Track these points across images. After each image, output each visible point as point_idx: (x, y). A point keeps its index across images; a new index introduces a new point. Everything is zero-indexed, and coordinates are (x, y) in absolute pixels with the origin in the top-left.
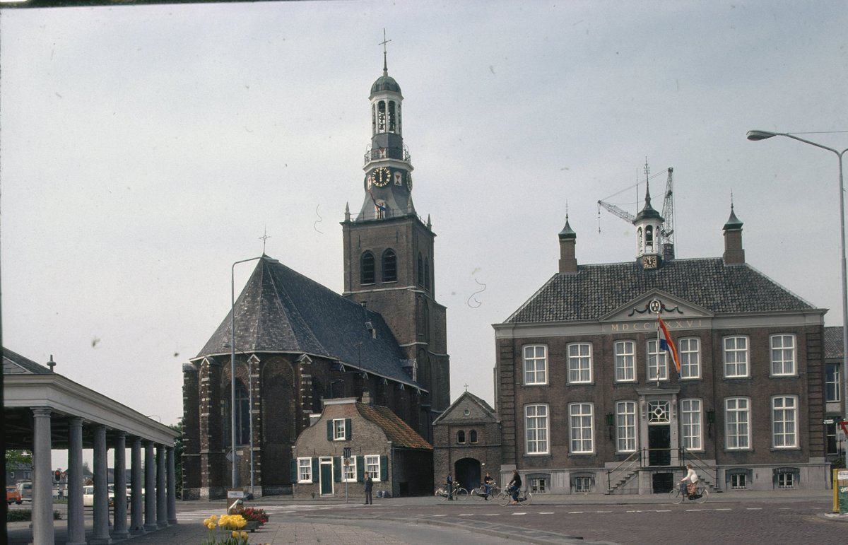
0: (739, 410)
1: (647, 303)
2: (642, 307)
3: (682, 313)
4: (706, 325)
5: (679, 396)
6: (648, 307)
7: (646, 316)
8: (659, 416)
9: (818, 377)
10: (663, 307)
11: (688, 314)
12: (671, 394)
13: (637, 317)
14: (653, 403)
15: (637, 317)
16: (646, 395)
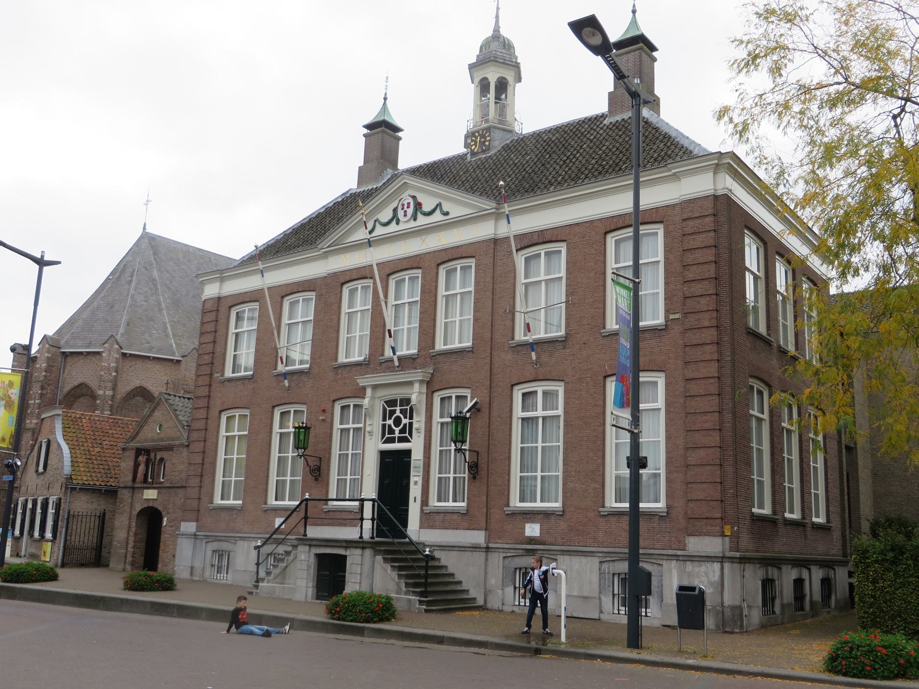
0: (538, 415)
1: (394, 205)
2: (385, 215)
3: (447, 214)
4: (484, 231)
5: (431, 387)
6: (395, 210)
7: (393, 228)
8: (397, 430)
9: (707, 323)
10: (418, 205)
11: (456, 212)
12: (410, 383)
13: (380, 231)
14: (391, 403)
15: (380, 231)
16: (375, 387)
